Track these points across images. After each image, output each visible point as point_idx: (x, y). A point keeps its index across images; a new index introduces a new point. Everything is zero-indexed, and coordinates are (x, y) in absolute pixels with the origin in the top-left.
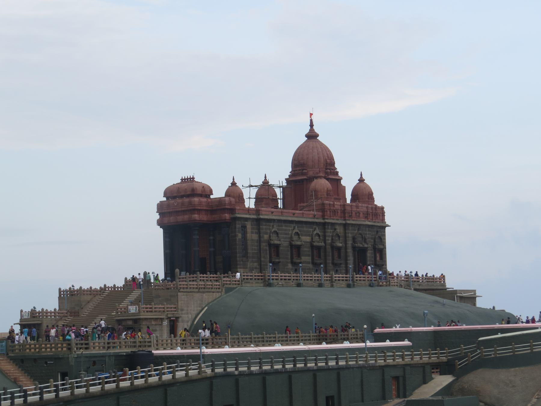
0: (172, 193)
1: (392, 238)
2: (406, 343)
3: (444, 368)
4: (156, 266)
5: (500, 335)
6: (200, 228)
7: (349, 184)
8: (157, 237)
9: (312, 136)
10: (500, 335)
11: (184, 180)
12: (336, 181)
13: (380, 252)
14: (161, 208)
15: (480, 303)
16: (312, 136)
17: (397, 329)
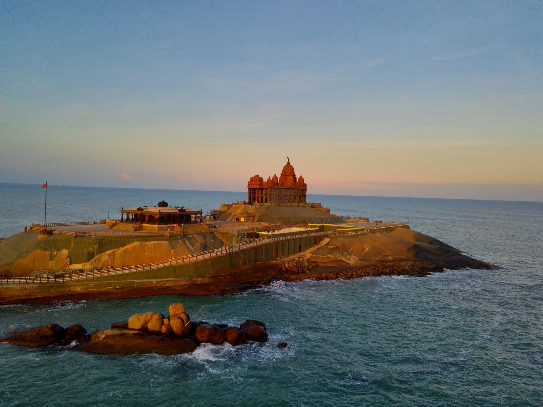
0: (252, 179)
1: (308, 192)
2: (317, 228)
3: (327, 236)
4: (247, 200)
5: (343, 229)
6: (258, 190)
7: (298, 177)
8: (247, 190)
9: (289, 163)
10: (343, 229)
11: (256, 176)
12: (294, 176)
13: (305, 196)
14: (249, 183)
15: (332, 213)
16: (289, 163)
17: (314, 224)
